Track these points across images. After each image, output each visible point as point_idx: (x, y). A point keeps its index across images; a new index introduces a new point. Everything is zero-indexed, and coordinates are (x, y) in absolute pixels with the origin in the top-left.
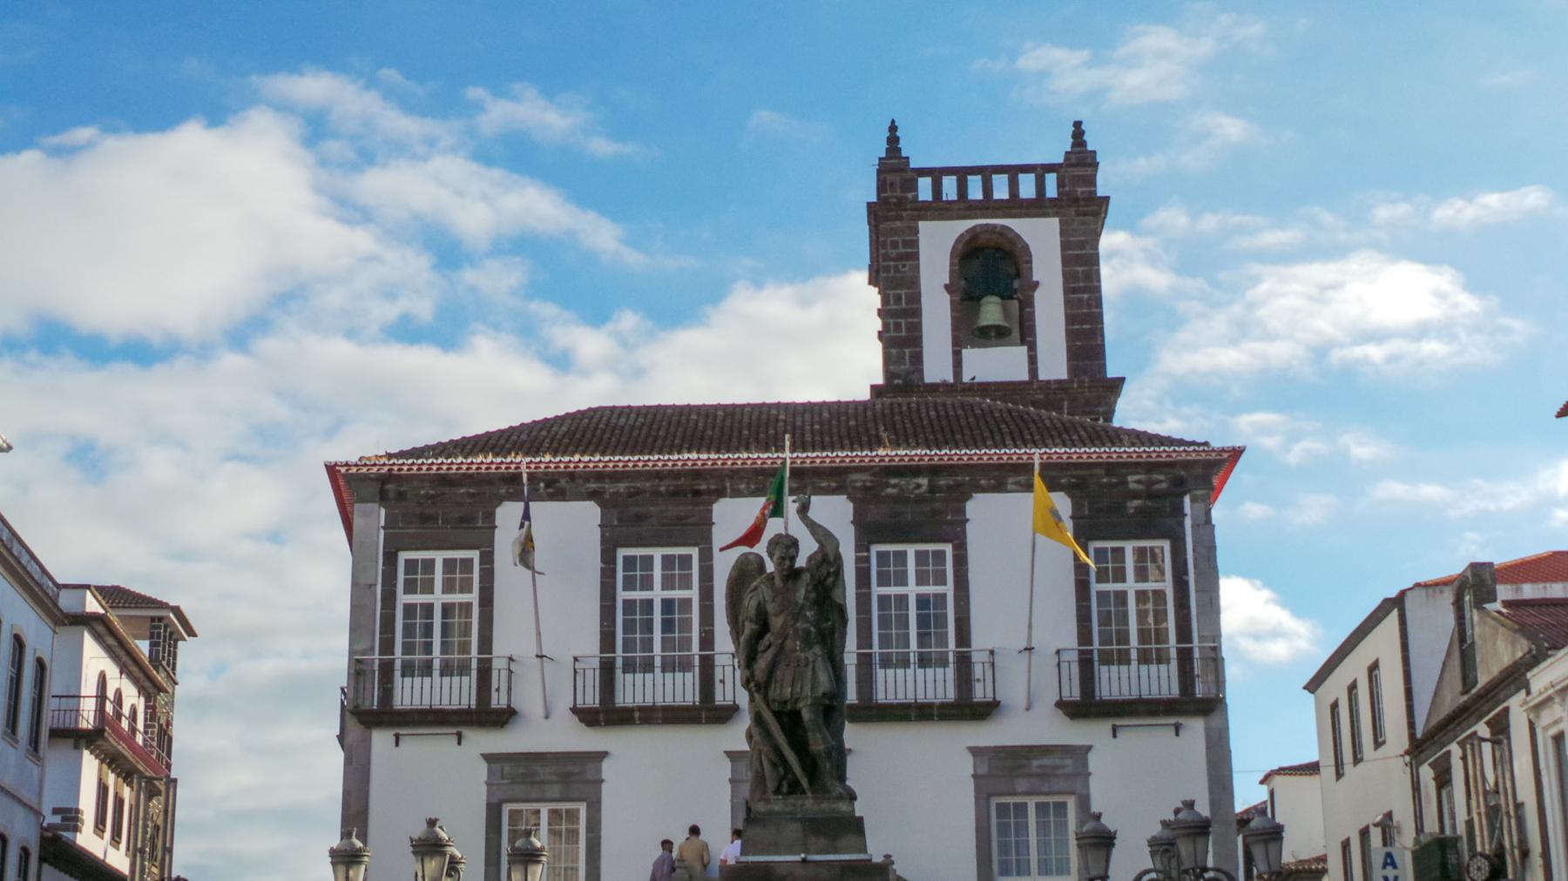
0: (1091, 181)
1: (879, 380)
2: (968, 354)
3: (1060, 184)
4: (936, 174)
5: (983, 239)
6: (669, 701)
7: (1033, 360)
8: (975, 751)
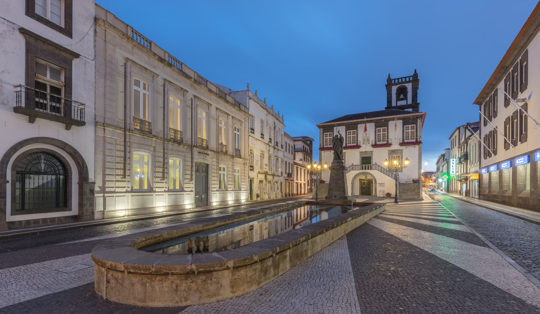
0: (417, 77)
1: (386, 106)
2: (398, 102)
3: (412, 78)
4: (395, 80)
7: (407, 102)
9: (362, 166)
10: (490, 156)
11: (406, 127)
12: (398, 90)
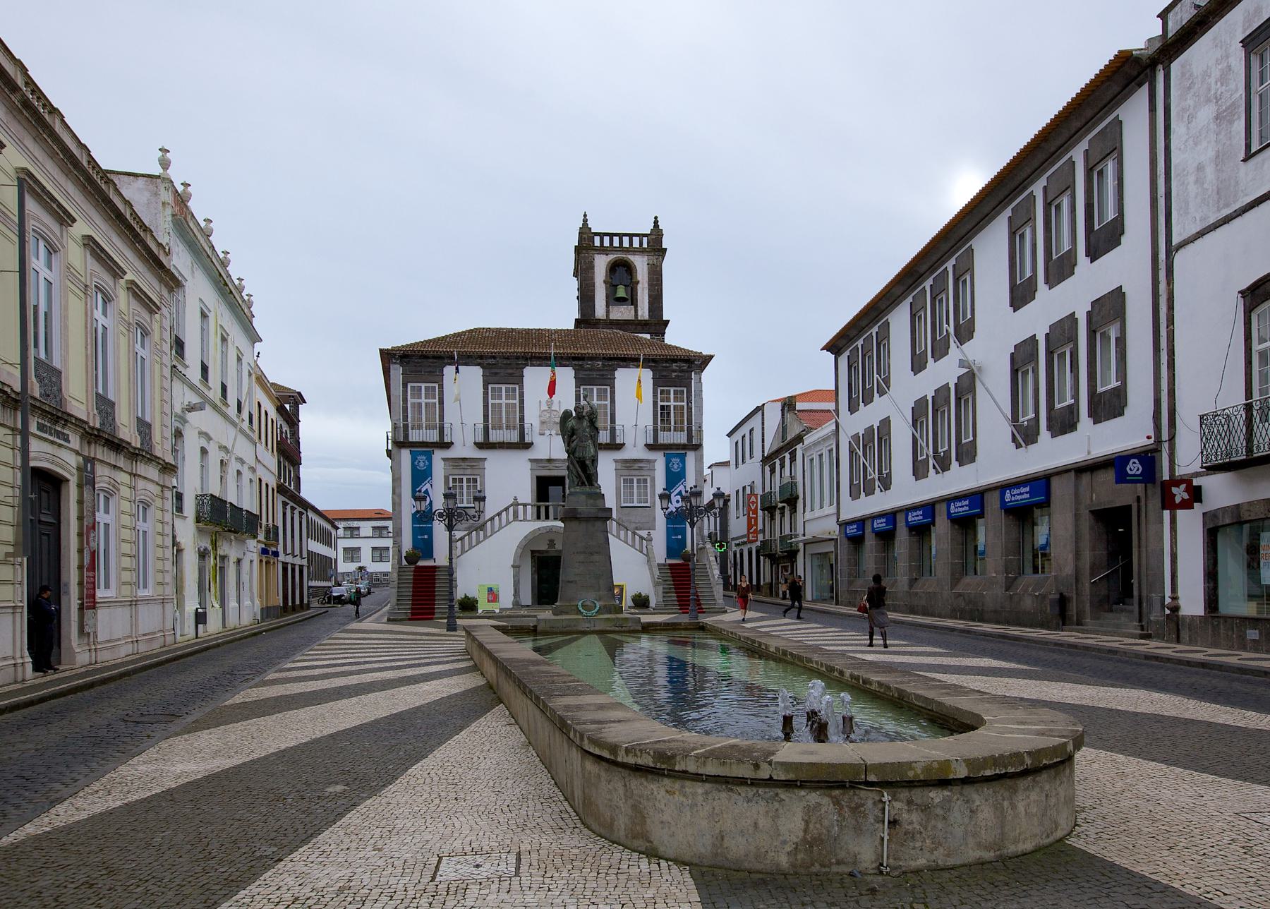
6: (509, 441)
8: (616, 461)
9: (539, 508)
10: (869, 491)
11: (662, 392)
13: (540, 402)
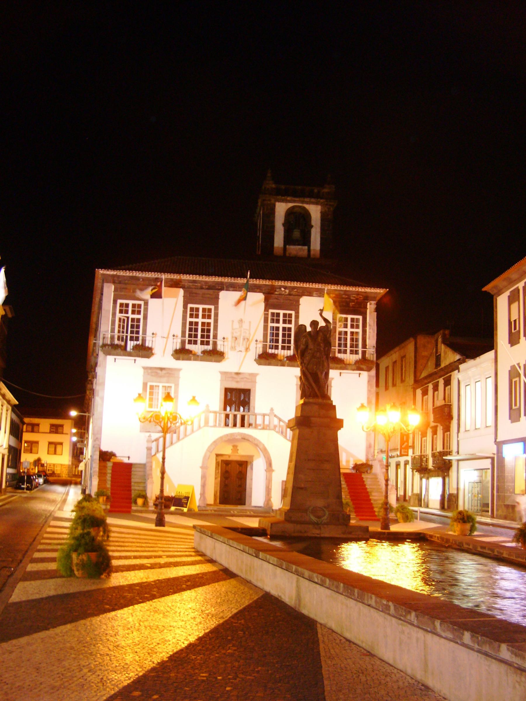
5: (296, 210)
12: (289, 213)
13: (233, 321)
